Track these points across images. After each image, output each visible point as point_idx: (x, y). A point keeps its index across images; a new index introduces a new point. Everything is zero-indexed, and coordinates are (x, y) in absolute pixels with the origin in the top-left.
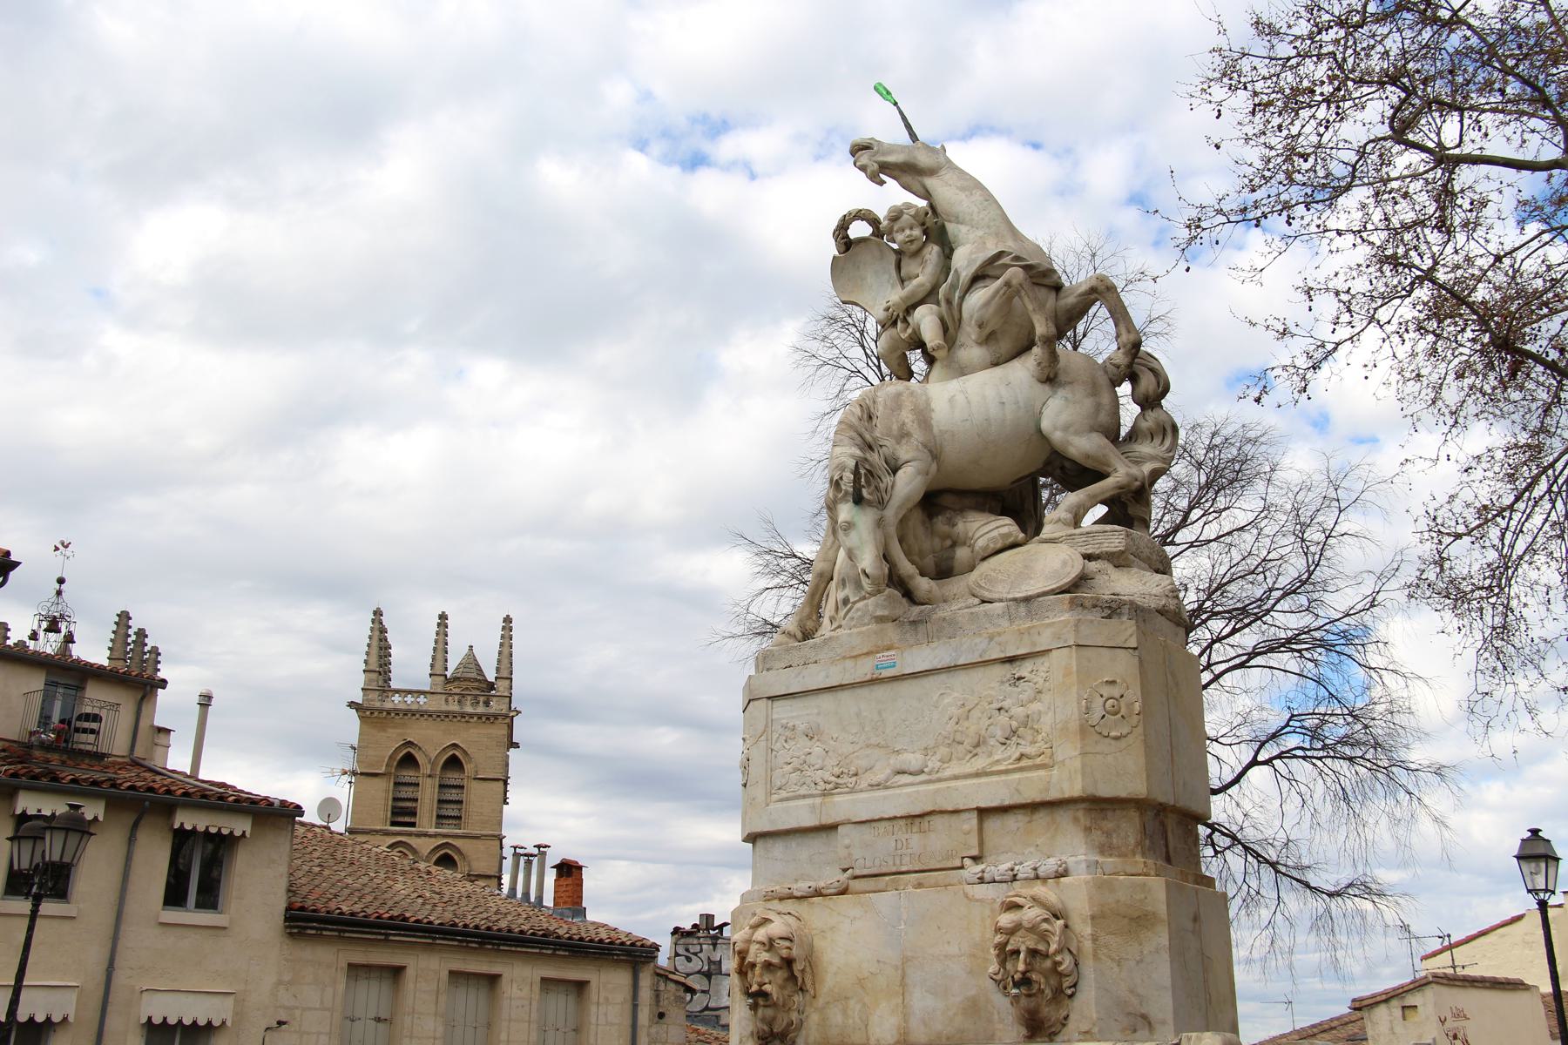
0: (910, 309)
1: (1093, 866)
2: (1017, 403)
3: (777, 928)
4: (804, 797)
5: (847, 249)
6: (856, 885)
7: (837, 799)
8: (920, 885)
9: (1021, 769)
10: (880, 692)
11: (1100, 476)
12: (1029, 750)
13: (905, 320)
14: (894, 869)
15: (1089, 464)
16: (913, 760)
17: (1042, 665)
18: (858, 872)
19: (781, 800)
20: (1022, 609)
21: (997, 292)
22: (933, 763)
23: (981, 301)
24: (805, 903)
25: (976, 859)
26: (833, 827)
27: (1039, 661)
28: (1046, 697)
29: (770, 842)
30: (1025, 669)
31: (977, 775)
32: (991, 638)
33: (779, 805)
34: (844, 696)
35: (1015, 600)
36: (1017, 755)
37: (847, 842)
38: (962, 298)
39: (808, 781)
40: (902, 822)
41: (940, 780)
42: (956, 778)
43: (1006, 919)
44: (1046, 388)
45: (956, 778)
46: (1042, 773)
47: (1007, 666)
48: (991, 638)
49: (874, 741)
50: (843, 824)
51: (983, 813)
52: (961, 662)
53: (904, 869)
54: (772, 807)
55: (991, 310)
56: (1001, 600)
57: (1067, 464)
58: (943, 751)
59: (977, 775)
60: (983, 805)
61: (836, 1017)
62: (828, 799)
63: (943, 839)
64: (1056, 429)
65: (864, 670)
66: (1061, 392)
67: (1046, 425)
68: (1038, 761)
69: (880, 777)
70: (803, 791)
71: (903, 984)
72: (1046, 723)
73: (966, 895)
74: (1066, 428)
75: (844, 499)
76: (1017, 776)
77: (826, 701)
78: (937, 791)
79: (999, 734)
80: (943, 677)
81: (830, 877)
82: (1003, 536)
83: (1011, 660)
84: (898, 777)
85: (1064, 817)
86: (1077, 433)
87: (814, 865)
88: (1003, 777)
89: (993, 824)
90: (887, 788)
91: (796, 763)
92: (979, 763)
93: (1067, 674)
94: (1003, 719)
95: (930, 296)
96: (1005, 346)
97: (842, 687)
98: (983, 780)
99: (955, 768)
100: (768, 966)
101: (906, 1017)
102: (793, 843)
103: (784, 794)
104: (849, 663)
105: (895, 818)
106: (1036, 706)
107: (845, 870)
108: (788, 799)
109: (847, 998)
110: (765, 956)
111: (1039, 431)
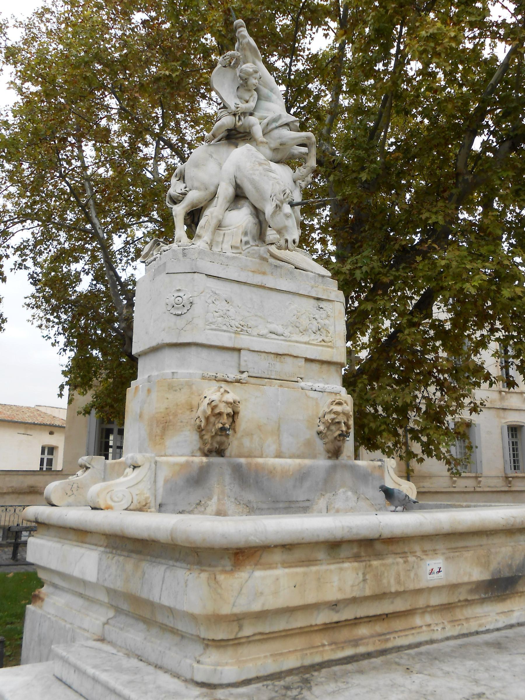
3: (230, 397)
4: (225, 331)
6: (253, 380)
7: (242, 336)
8: (281, 386)
9: (323, 346)
12: (326, 339)
14: (268, 377)
16: (279, 329)
18: (251, 374)
19: (212, 329)
20: (320, 279)
21: (301, 137)
22: (287, 333)
24: (231, 385)
26: (239, 350)
28: (332, 320)
29: (200, 349)
30: (323, 304)
31: (305, 343)
32: (312, 287)
33: (210, 332)
35: (319, 274)
36: (321, 339)
37: (246, 358)
39: (228, 324)
40: (273, 356)
41: (290, 341)
42: (297, 342)
45: (297, 342)
46: (329, 349)
47: (316, 301)
49: (259, 314)
50: (244, 349)
51: (307, 360)
52: (300, 293)
53: (272, 377)
54: (206, 331)
58: (290, 328)
59: (305, 343)
60: (308, 357)
61: (246, 442)
62: (238, 336)
63: (289, 367)
68: (329, 344)
69: (264, 331)
70: (224, 328)
71: (279, 429)
73: (306, 395)
76: (321, 348)
78: (289, 346)
79: (314, 329)
80: (290, 296)
83: (318, 299)
84: (271, 334)
88: (315, 347)
90: (266, 338)
91: (221, 313)
92: (305, 339)
94: (315, 322)
96: (279, 157)
98: (307, 346)
99: (295, 337)
101: (280, 445)
102: (214, 353)
103: (213, 327)
104: (251, 274)
105: (270, 353)
106: (327, 322)
107: (243, 372)
108: (215, 330)
109: (252, 434)
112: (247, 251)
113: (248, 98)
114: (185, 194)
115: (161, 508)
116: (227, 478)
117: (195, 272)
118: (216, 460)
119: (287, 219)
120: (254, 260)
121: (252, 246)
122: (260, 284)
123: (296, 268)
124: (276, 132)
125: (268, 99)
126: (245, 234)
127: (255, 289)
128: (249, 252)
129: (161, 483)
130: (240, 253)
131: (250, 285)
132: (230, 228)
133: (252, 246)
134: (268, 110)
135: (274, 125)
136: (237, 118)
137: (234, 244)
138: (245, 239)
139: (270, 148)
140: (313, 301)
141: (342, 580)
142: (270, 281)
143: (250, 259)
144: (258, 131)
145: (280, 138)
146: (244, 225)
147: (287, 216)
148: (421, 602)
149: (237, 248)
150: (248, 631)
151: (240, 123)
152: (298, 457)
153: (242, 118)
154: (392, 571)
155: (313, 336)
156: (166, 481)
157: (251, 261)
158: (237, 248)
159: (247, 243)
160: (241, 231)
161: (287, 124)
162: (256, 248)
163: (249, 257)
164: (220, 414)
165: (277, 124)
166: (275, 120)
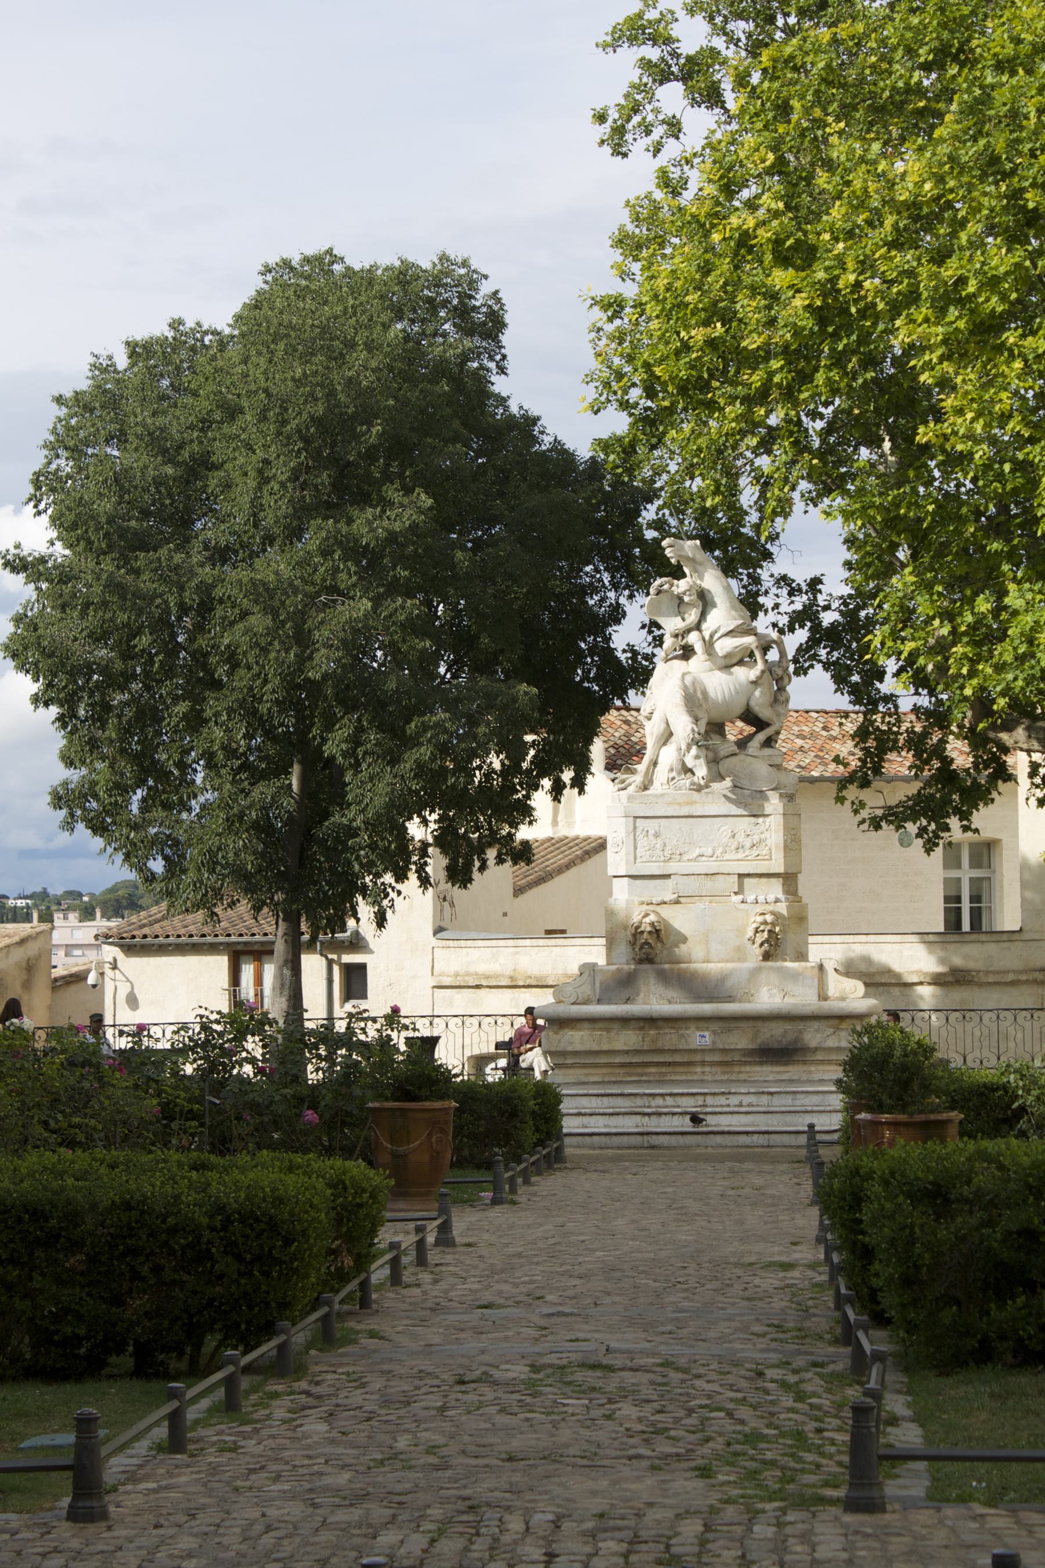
0: (689, 631)
1: (787, 900)
3: (652, 918)
15: (765, 719)
25: (736, 893)
26: (667, 876)
43: (760, 919)
51: (740, 876)
67: (752, 703)
72: (768, 842)
79: (748, 844)
81: (669, 897)
85: (773, 880)
87: (665, 891)
89: (747, 880)
92: (740, 856)
100: (650, 932)
101: (708, 952)
110: (649, 929)
115: (599, 1002)
116: (652, 981)
118: (647, 966)
126: (672, 770)
129: (598, 985)
138: (672, 775)
141: (627, 1039)
144: (698, 647)
148: (698, 1058)
150: (569, 1061)
152: (727, 961)
154: (669, 1038)
155: (747, 853)
156: (601, 984)
161: (731, 631)
164: (642, 932)
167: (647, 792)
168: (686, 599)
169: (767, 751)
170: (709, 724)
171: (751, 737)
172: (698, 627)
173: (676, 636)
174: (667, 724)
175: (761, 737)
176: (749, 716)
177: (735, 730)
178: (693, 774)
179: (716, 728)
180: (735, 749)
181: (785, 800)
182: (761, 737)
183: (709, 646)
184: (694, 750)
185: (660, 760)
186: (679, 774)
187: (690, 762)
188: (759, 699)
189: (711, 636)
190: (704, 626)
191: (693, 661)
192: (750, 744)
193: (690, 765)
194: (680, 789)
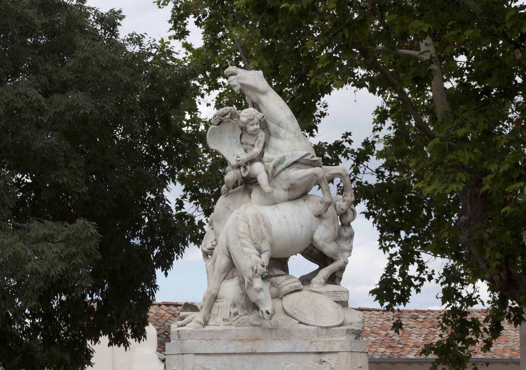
0: (251, 161)
2: (307, 226)
5: (219, 124)
10: (254, 358)
11: (332, 261)
13: (245, 169)
17: (334, 357)
20: (324, 331)
23: (299, 177)
27: (332, 355)
30: (326, 358)
32: (311, 343)
34: (236, 357)
35: (322, 327)
38: (283, 169)
44: (318, 219)
47: (317, 355)
48: (311, 343)
52: (297, 351)
55: (302, 182)
56: (314, 326)
57: (315, 251)
64: (321, 239)
65: (247, 347)
66: (324, 222)
67: (316, 237)
74: (325, 240)
75: (257, 277)
77: (225, 358)
80: (286, 356)
82: (296, 287)
86: (330, 242)
93: (347, 362)
95: (260, 158)
96: (298, 193)
97: (235, 354)
104: (239, 344)
111: (312, 239)
112: (236, 321)
113: (253, 143)
114: (213, 249)
117: (183, 354)
119: (258, 293)
120: (245, 328)
121: (241, 316)
122: (250, 351)
123: (300, 323)
124: (284, 173)
125: (277, 136)
126: (234, 305)
127: (246, 357)
128: (239, 322)
130: (231, 325)
131: (240, 354)
132: (224, 300)
133: (241, 316)
134: (276, 149)
135: (279, 169)
136: (242, 169)
137: (224, 317)
138: (233, 311)
139: (285, 190)
140: (313, 356)
142: (261, 347)
143: (242, 328)
144: (263, 178)
145: (288, 180)
146: (232, 298)
147: (259, 290)
149: (228, 320)
151: (247, 173)
153: (248, 167)
157: (242, 330)
158: (228, 320)
159: (236, 314)
160: (230, 302)
161: (295, 163)
162: (245, 317)
163: (240, 326)
165: (283, 166)
166: (280, 162)
167: (207, 328)
168: (251, 128)
169: (331, 288)
170: (271, 259)
171: (315, 273)
172: (260, 158)
173: (239, 167)
174: (230, 257)
175: (325, 272)
176: (313, 253)
177: (299, 265)
178: (258, 309)
179: (279, 263)
180: (298, 284)
181: (352, 337)
182: (325, 272)
183: (273, 176)
184: (258, 283)
185: (221, 294)
186: (243, 308)
187: (254, 296)
188: (323, 235)
189: (274, 167)
190: (266, 155)
191: (255, 194)
192: (314, 280)
193: (253, 300)
194: (243, 324)
